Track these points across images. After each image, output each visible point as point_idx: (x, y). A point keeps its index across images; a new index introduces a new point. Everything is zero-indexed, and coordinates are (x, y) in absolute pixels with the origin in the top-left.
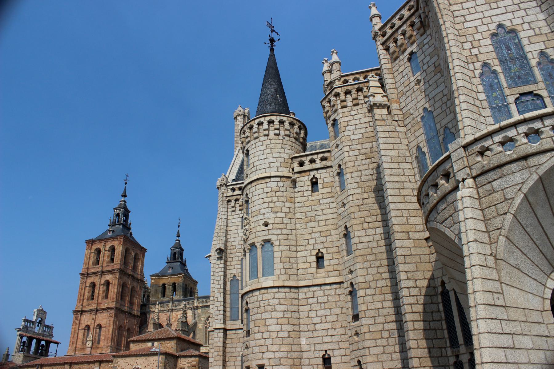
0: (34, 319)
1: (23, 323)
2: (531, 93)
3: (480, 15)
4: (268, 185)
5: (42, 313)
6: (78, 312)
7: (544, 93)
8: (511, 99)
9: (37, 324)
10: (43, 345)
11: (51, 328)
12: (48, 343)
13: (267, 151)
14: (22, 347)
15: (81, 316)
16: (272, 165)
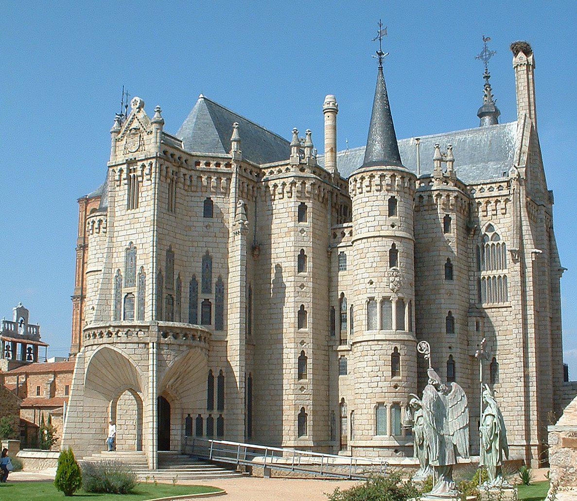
0: (15, 321)
1: (2, 326)
2: (131, 293)
3: (124, 233)
4: (97, 277)
5: (23, 312)
6: (78, 298)
7: (136, 294)
8: (123, 296)
9: (19, 325)
10: (30, 349)
11: (37, 327)
12: (36, 346)
13: (98, 247)
14: (6, 352)
15: (82, 304)
16: (100, 259)
